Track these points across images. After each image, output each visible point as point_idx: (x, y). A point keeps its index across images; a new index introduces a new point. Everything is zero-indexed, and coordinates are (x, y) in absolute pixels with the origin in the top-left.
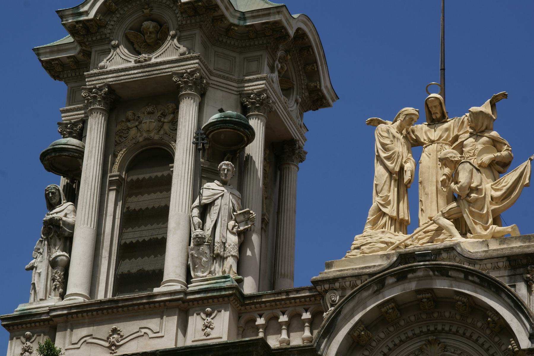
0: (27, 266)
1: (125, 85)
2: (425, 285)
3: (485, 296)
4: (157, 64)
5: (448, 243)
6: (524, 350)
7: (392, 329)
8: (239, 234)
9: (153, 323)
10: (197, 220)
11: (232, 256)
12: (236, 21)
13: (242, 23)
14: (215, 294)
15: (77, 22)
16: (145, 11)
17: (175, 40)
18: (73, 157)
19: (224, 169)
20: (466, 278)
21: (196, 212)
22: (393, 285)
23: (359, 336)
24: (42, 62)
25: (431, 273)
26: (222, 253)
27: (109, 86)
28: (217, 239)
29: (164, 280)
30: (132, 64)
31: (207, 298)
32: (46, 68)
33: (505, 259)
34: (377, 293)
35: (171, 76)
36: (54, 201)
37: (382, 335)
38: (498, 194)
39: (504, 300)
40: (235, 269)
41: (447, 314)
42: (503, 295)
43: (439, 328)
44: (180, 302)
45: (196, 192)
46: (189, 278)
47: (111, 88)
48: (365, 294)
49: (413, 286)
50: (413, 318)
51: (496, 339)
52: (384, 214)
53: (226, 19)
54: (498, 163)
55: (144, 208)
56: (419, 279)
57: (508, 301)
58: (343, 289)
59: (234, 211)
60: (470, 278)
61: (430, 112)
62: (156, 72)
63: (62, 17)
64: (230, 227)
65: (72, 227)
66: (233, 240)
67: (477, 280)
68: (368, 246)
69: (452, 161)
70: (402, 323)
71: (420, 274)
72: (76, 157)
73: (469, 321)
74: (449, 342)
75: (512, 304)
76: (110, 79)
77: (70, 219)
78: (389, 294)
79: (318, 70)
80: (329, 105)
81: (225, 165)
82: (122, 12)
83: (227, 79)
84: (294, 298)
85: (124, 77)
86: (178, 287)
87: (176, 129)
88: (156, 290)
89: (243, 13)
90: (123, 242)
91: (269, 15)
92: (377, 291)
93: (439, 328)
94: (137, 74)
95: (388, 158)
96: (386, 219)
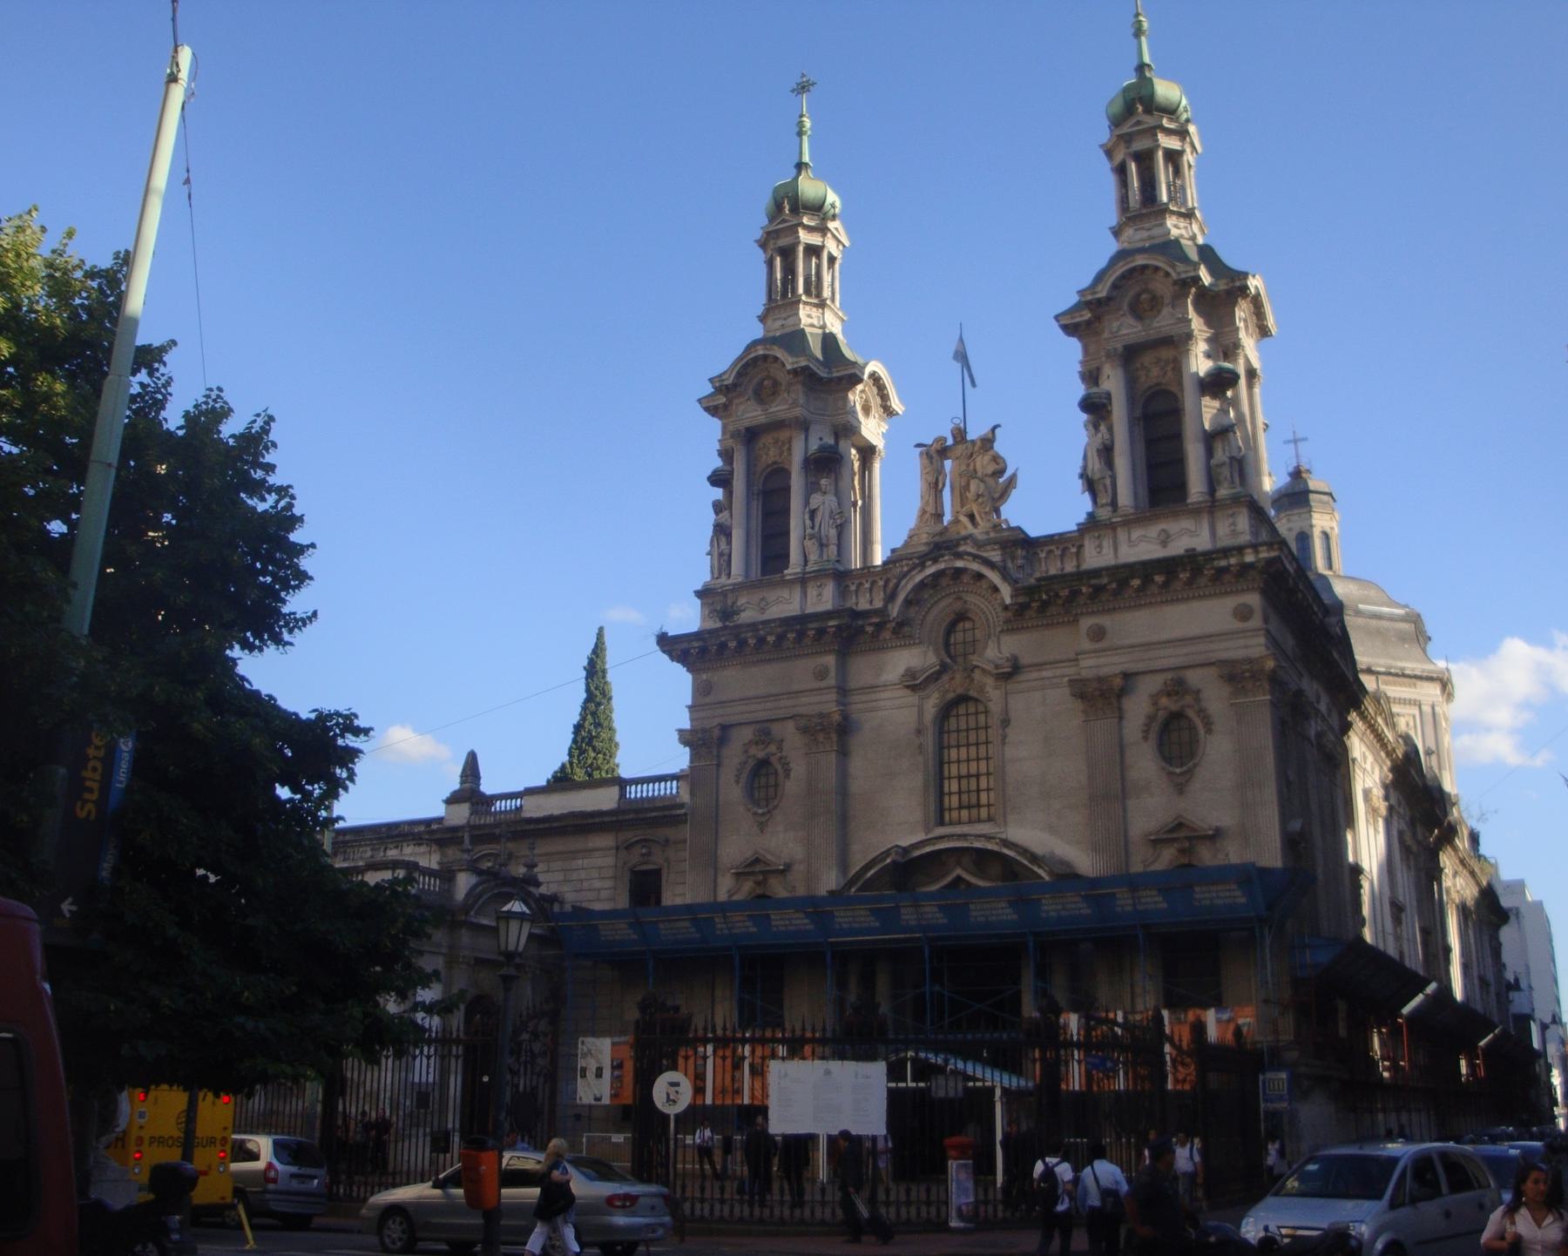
2: (950, 565)
5: (964, 533)
8: (837, 527)
9: (785, 593)
10: (808, 522)
12: (826, 375)
17: (786, 395)
20: (974, 560)
21: (807, 516)
22: (930, 566)
30: (759, 413)
34: (920, 571)
40: (835, 553)
45: (807, 503)
46: (806, 561)
47: (748, 430)
48: (913, 573)
56: (945, 561)
58: (902, 566)
65: (730, 528)
66: (833, 532)
71: (946, 558)
74: (968, 599)
76: (747, 424)
77: (729, 524)
83: (824, 415)
85: (755, 423)
86: (799, 570)
88: (786, 572)
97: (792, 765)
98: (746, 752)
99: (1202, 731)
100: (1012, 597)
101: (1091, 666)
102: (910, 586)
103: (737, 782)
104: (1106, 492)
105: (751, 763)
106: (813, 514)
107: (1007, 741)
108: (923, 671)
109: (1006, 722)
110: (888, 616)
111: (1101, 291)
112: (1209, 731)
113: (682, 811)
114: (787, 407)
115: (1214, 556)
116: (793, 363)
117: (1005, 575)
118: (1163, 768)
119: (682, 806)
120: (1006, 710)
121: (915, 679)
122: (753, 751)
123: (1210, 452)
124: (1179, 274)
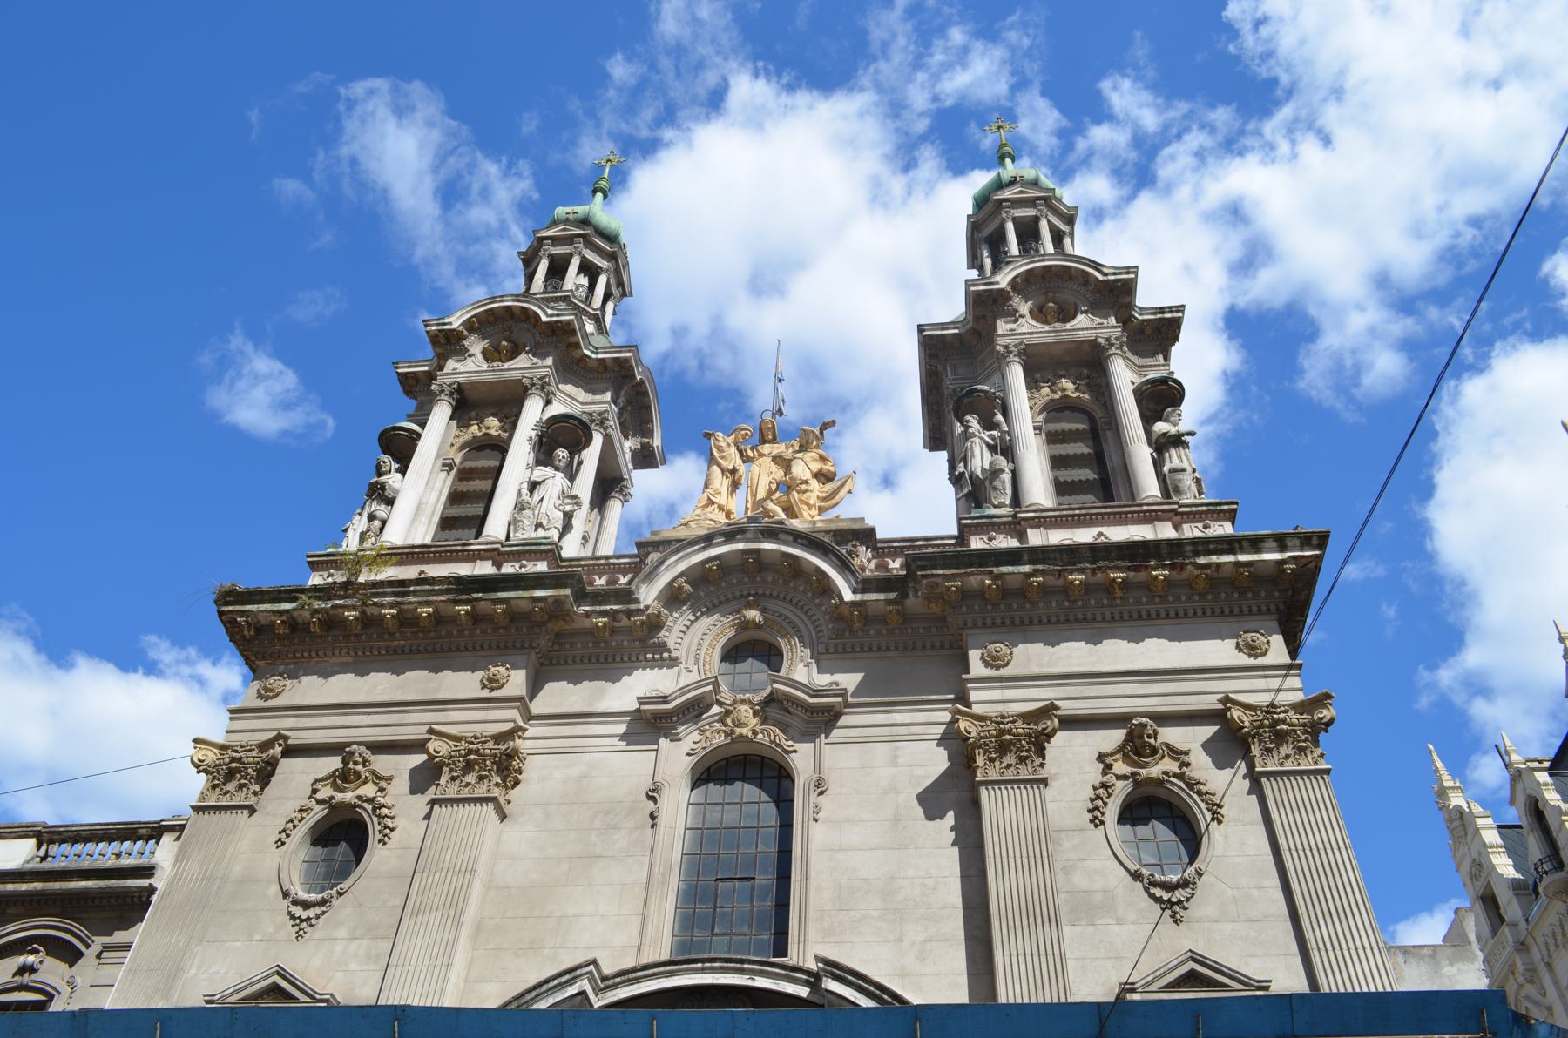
0: (343, 528)
1: (474, 385)
3: (812, 554)
4: (509, 370)
6: (847, 603)
7: (712, 589)
11: (556, 528)
13: (594, 356)
14: (533, 548)
15: (440, 331)
16: (506, 333)
18: (411, 437)
19: (559, 456)
23: (680, 587)
24: (398, 373)
25: (760, 536)
26: (545, 524)
27: (459, 384)
28: (543, 510)
29: (483, 534)
30: (485, 368)
31: (524, 552)
32: (401, 382)
33: (832, 534)
35: (521, 380)
36: (384, 470)
37: (702, 594)
38: (824, 495)
39: (831, 560)
41: (770, 579)
42: (831, 556)
43: (760, 591)
44: (496, 553)
46: (508, 537)
49: (741, 546)
50: (735, 581)
51: (817, 601)
52: (713, 503)
53: (580, 348)
54: (823, 475)
55: (471, 490)
57: (834, 559)
59: (563, 493)
60: (799, 540)
61: (762, 434)
62: (507, 376)
63: (426, 326)
64: (557, 505)
67: (805, 542)
68: (695, 522)
69: (785, 459)
70: (723, 584)
71: (749, 535)
72: (414, 439)
73: (792, 585)
75: (839, 563)
76: (461, 379)
77: (396, 485)
78: (714, 552)
79: (653, 430)
80: (657, 467)
81: (562, 453)
82: (483, 331)
84: (614, 564)
87: (515, 429)
89: (596, 348)
90: (444, 516)
91: (620, 352)
92: (704, 547)
93: (760, 591)
94: (488, 376)
95: (722, 458)
96: (716, 505)
97: (400, 822)
98: (315, 791)
99: (1203, 815)
100: (855, 591)
101: (984, 699)
102: (681, 567)
103: (281, 843)
104: (1004, 490)
105: (318, 812)
106: (533, 486)
107: (820, 816)
108: (683, 690)
109: (820, 786)
110: (637, 601)
111: (997, 283)
112: (1217, 818)
113: (144, 882)
114: (526, 366)
115: (1211, 546)
116: (552, 316)
117: (844, 566)
118: (1136, 876)
119: (148, 871)
120: (818, 767)
121: (666, 703)
122: (325, 792)
123: (1158, 464)
124: (1106, 274)
